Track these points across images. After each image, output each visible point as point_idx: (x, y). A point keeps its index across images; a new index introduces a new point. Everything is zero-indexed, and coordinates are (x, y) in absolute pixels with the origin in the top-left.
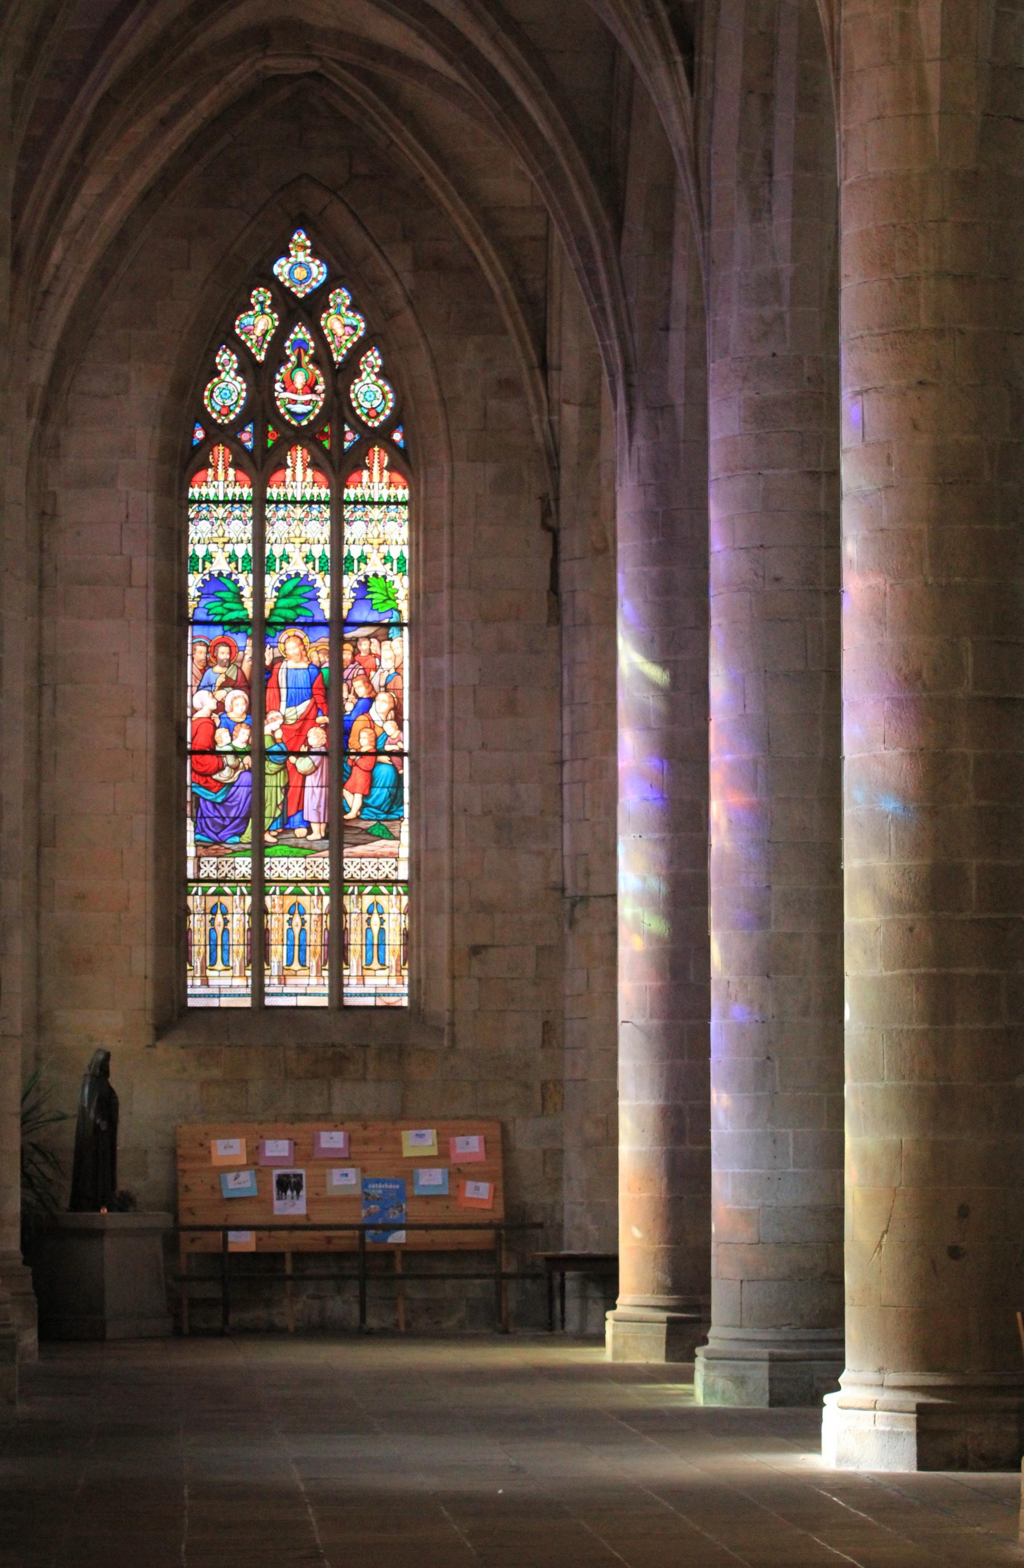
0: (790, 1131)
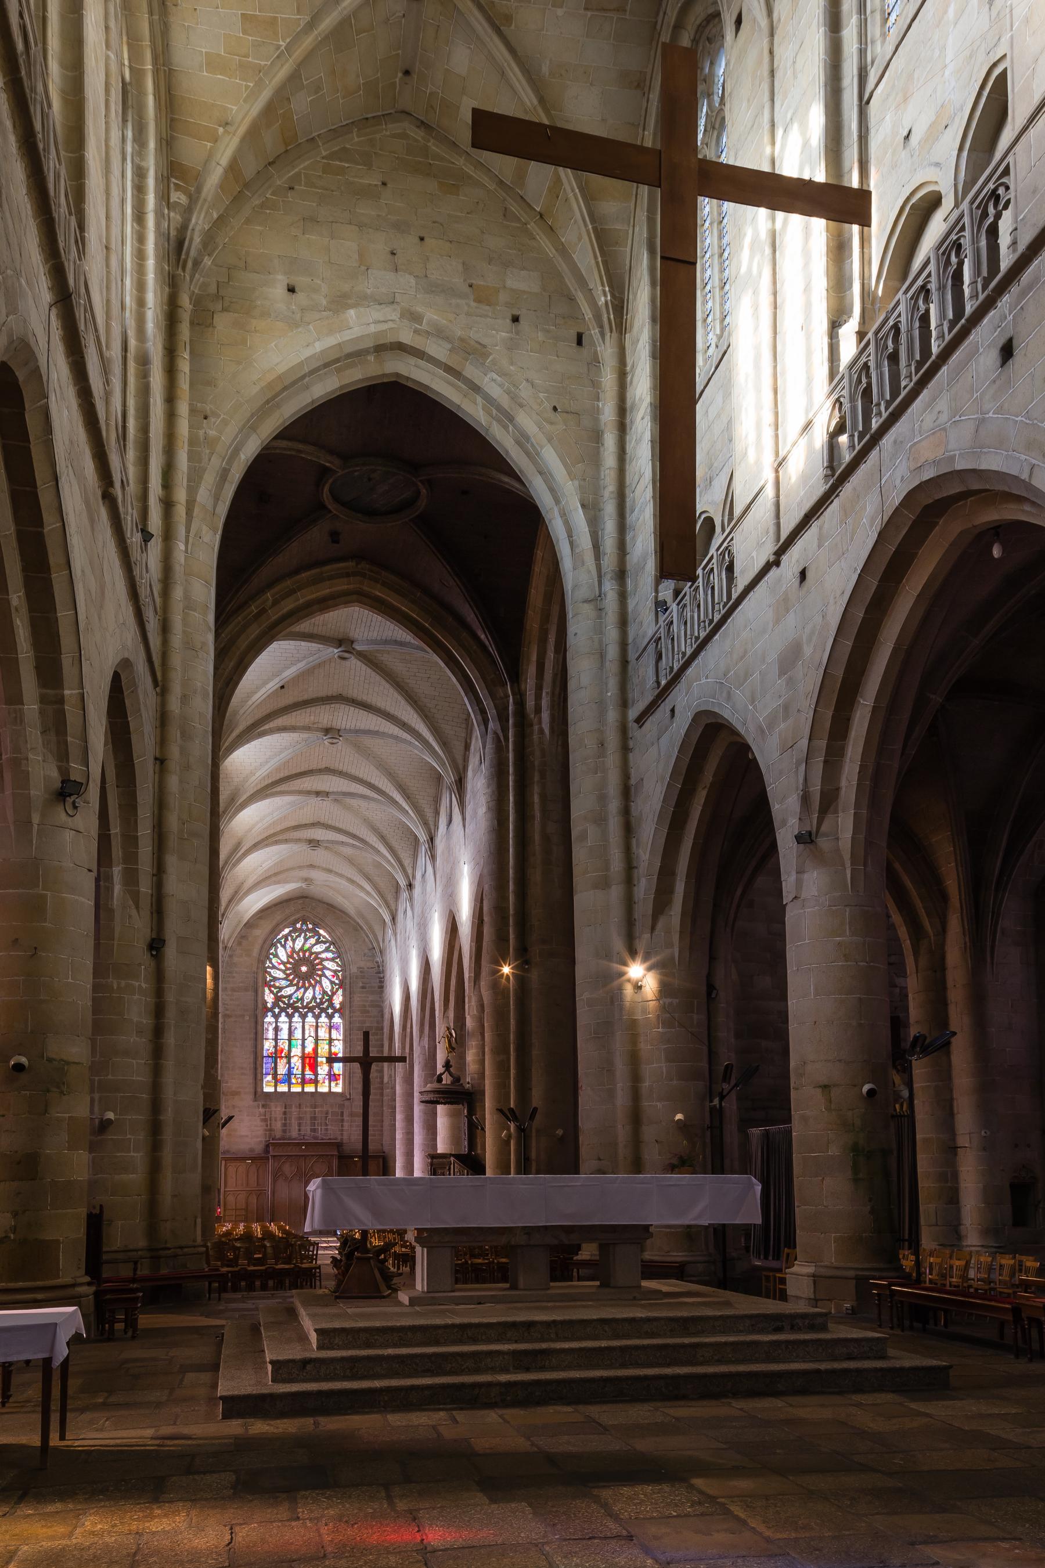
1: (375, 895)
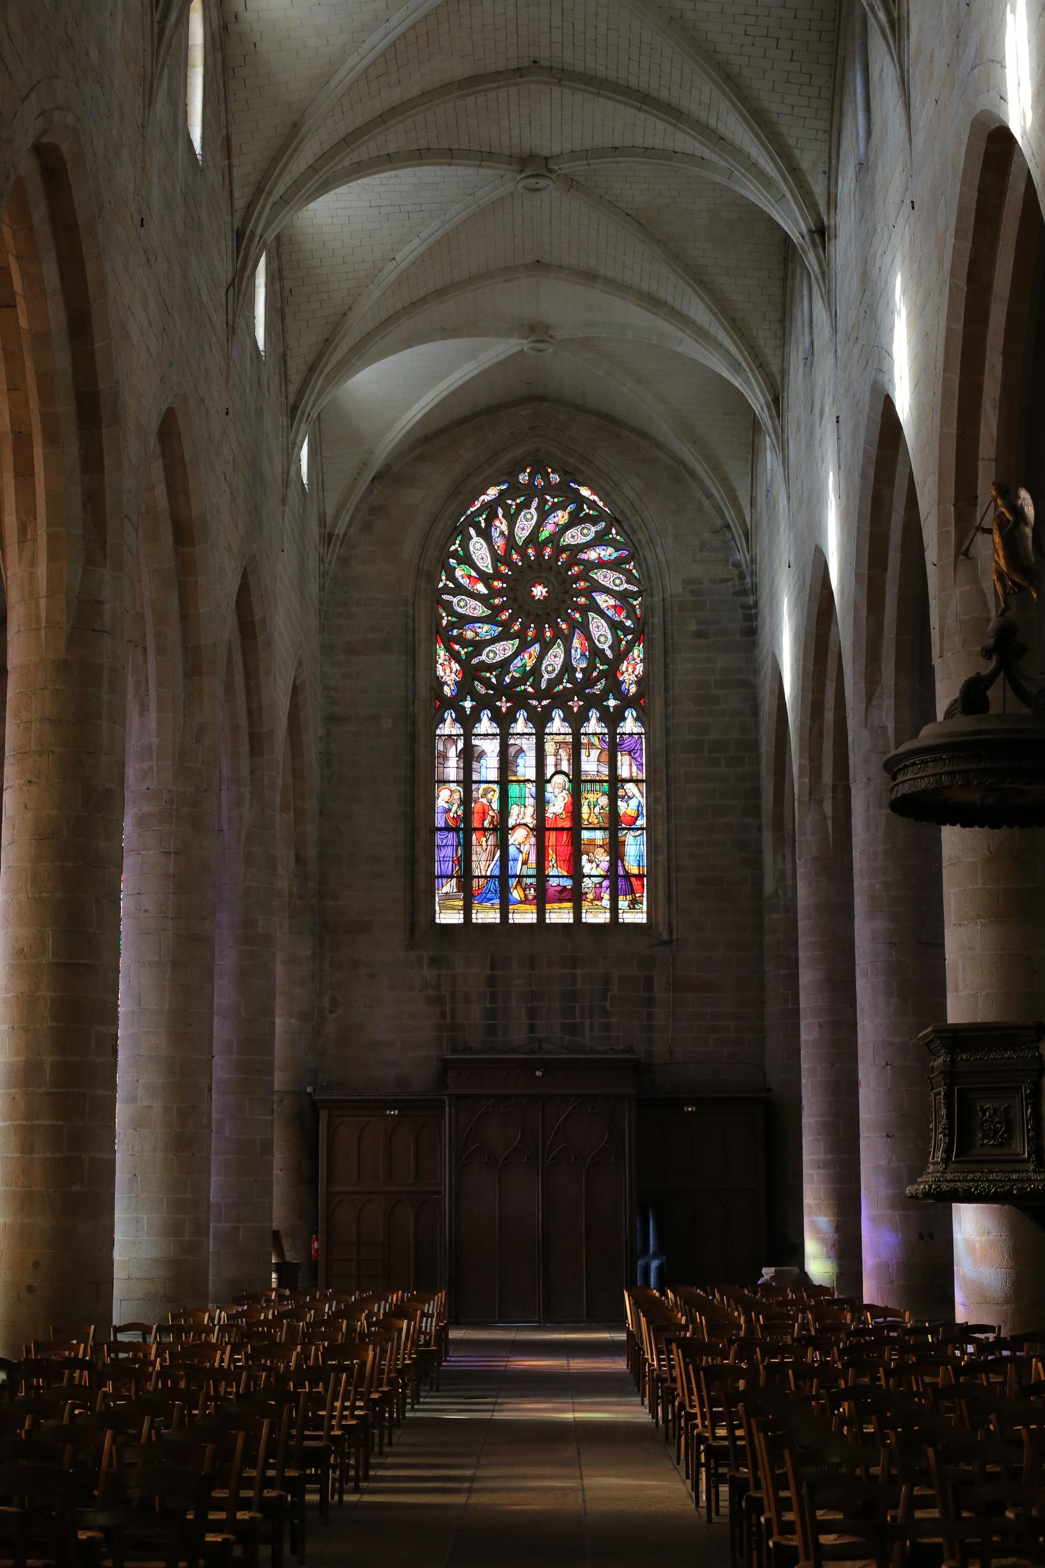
0: (145, 1216)
1: (728, 343)
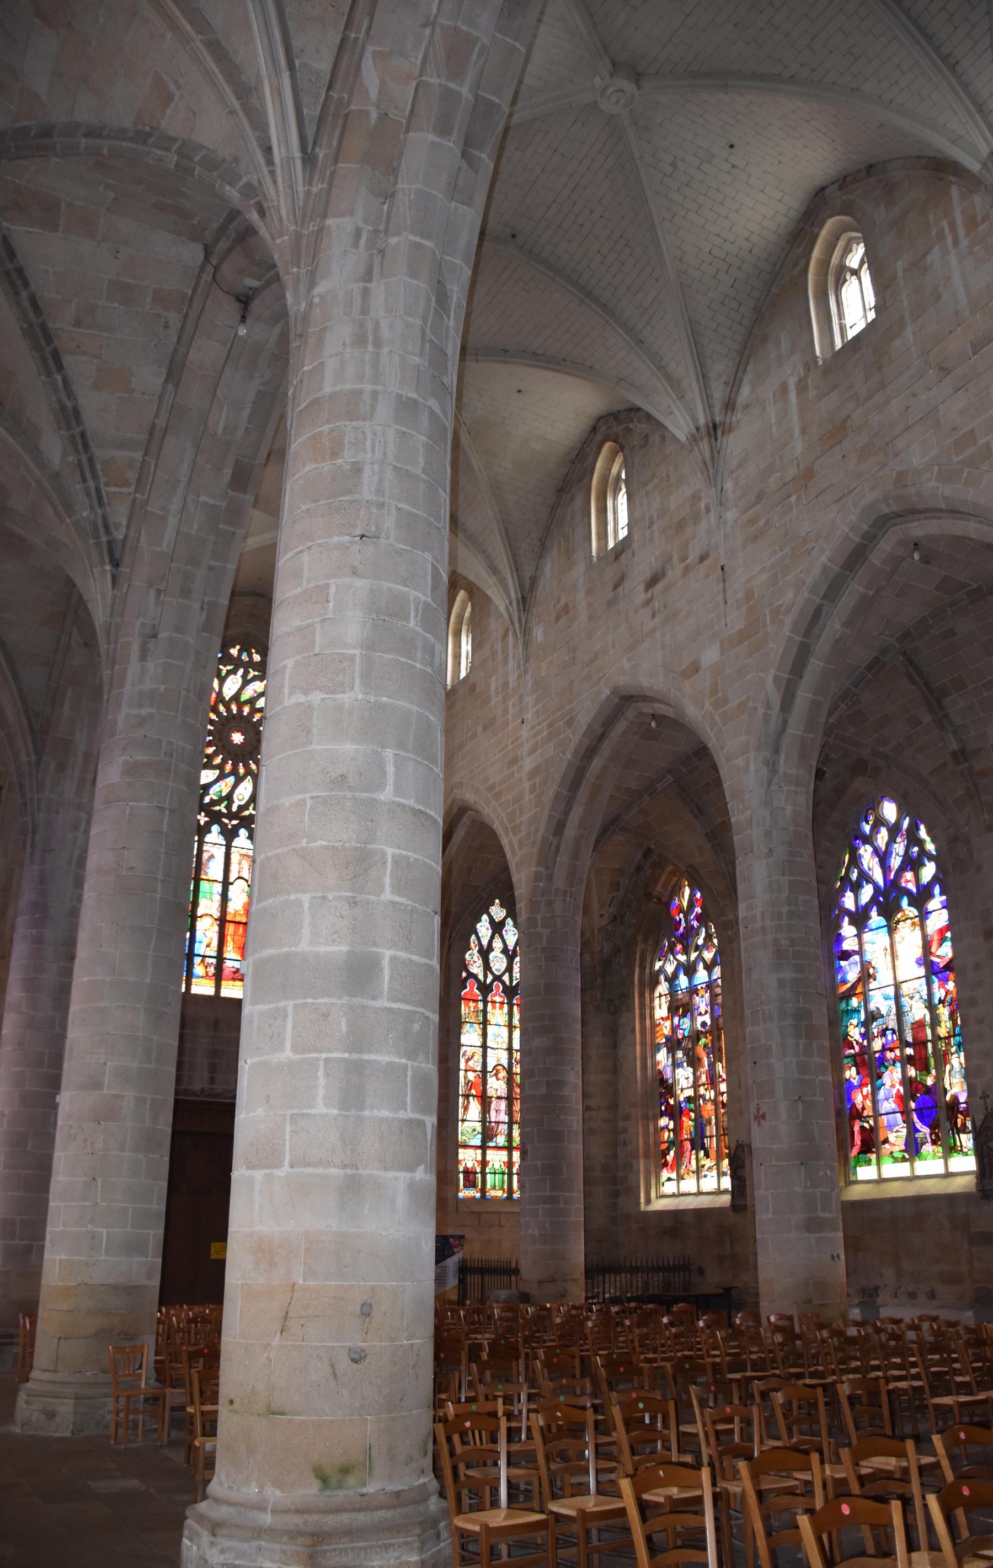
0: (105, 1230)
